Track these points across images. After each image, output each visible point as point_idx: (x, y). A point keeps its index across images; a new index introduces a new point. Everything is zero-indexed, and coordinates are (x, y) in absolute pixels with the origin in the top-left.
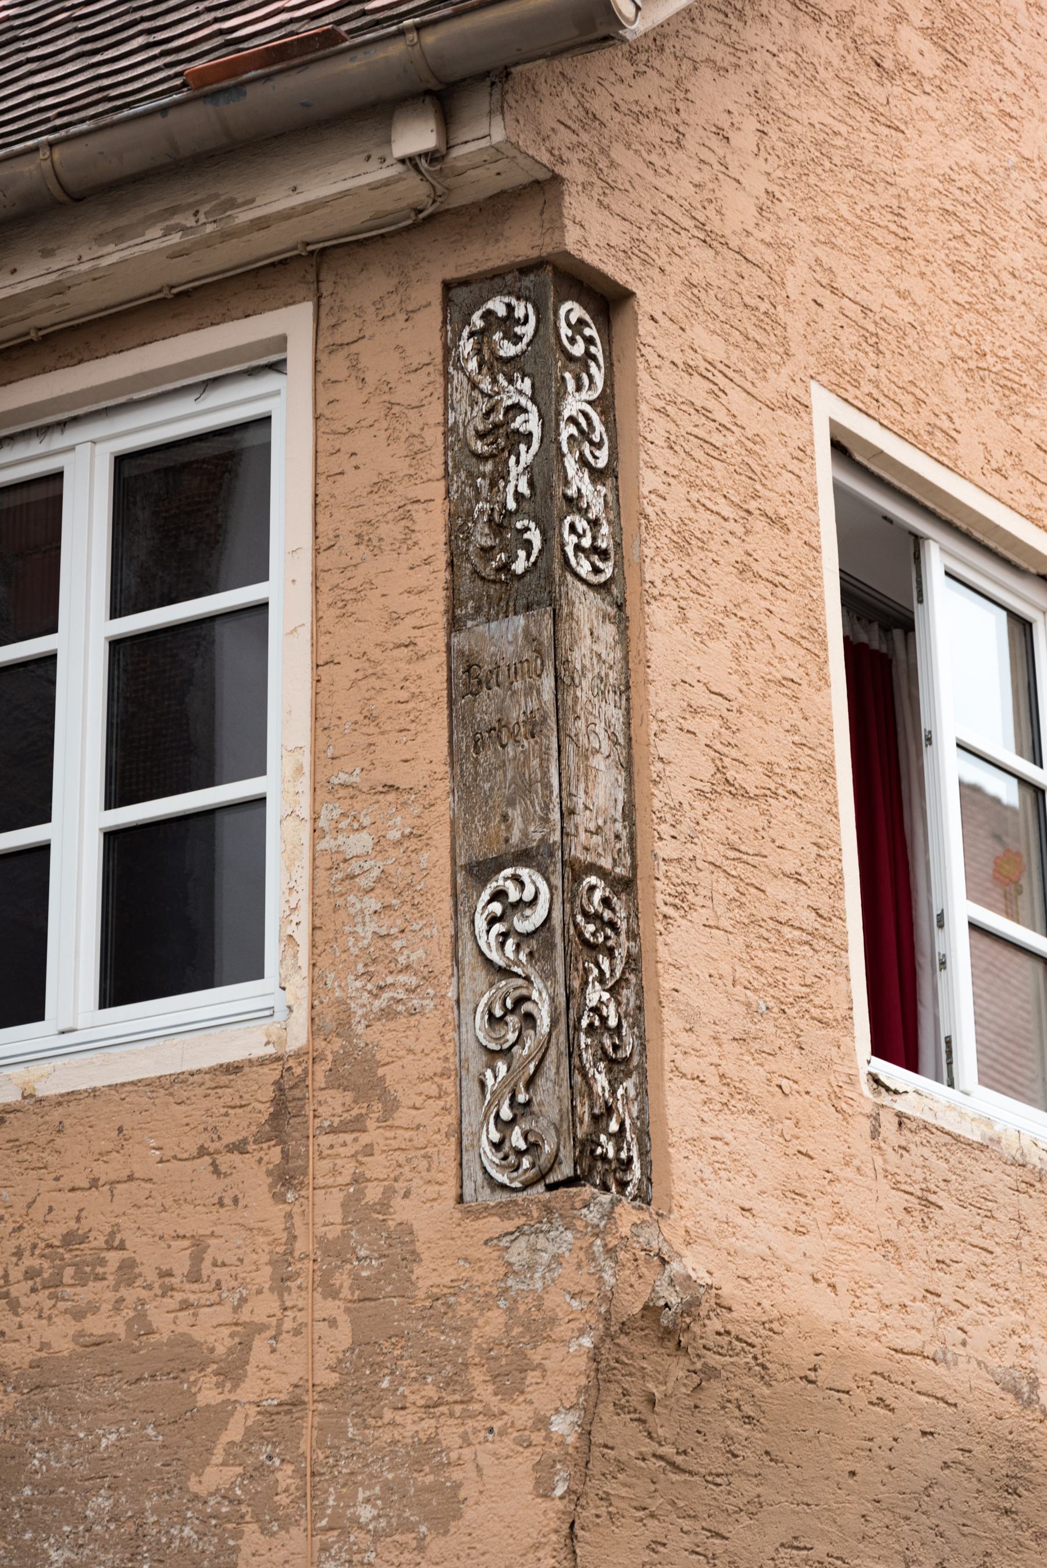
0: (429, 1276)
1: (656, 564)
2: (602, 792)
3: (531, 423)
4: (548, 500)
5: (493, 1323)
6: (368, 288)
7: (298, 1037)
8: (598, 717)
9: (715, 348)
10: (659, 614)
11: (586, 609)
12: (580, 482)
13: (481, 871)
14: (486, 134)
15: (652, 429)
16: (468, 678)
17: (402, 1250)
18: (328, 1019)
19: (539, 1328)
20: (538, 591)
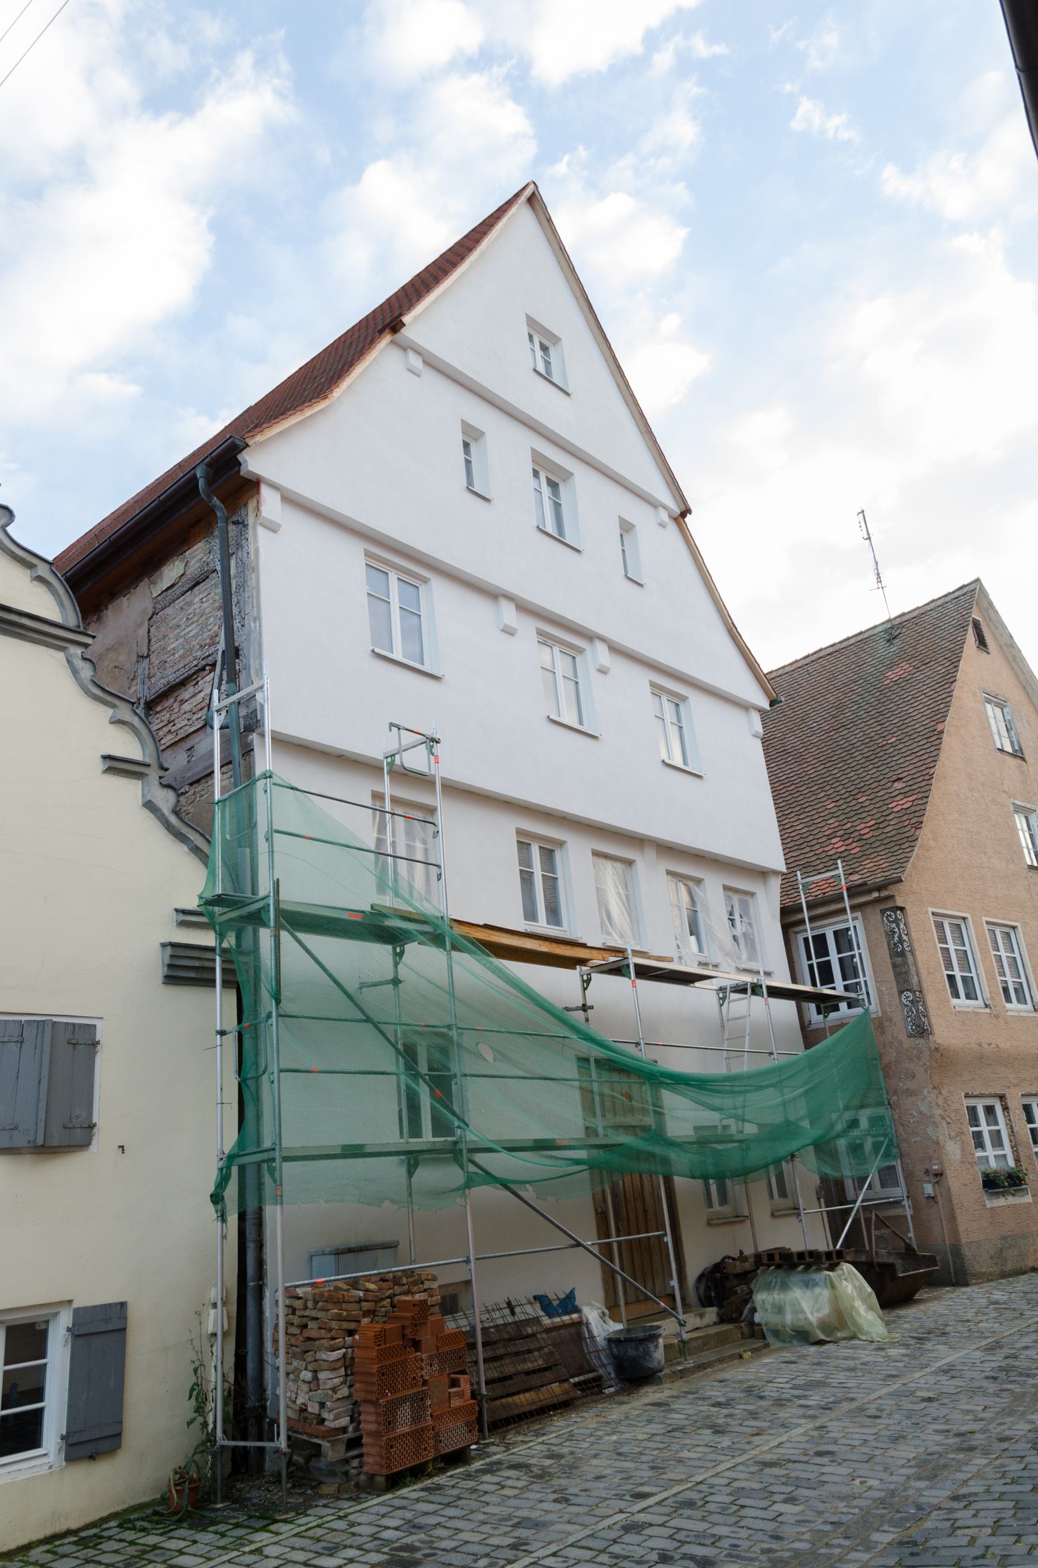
0: (906, 1045)
1: (916, 945)
2: (915, 980)
3: (896, 930)
4: (901, 941)
5: (915, 1052)
6: (869, 910)
7: (880, 1014)
8: (913, 969)
9: (915, 909)
10: (917, 953)
11: (908, 955)
12: (905, 938)
13: (901, 992)
14: (884, 893)
15: (911, 926)
16: (895, 966)
17: (901, 1043)
18: (884, 1012)
19: (922, 1052)
20: (902, 954)
